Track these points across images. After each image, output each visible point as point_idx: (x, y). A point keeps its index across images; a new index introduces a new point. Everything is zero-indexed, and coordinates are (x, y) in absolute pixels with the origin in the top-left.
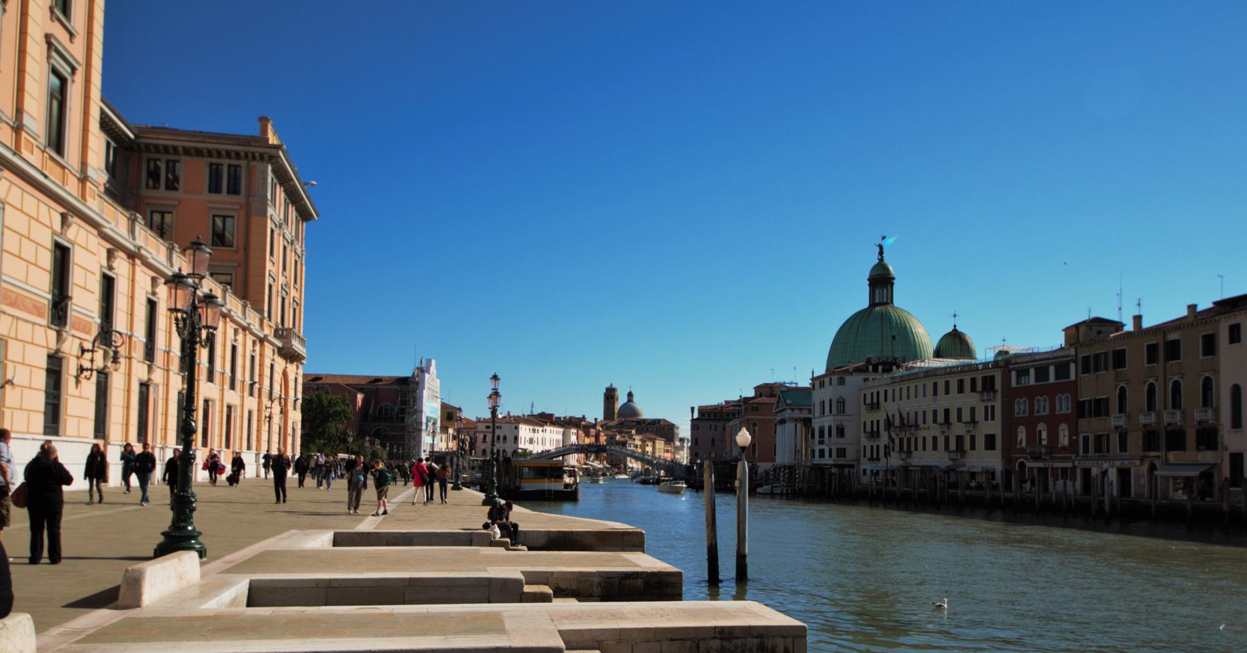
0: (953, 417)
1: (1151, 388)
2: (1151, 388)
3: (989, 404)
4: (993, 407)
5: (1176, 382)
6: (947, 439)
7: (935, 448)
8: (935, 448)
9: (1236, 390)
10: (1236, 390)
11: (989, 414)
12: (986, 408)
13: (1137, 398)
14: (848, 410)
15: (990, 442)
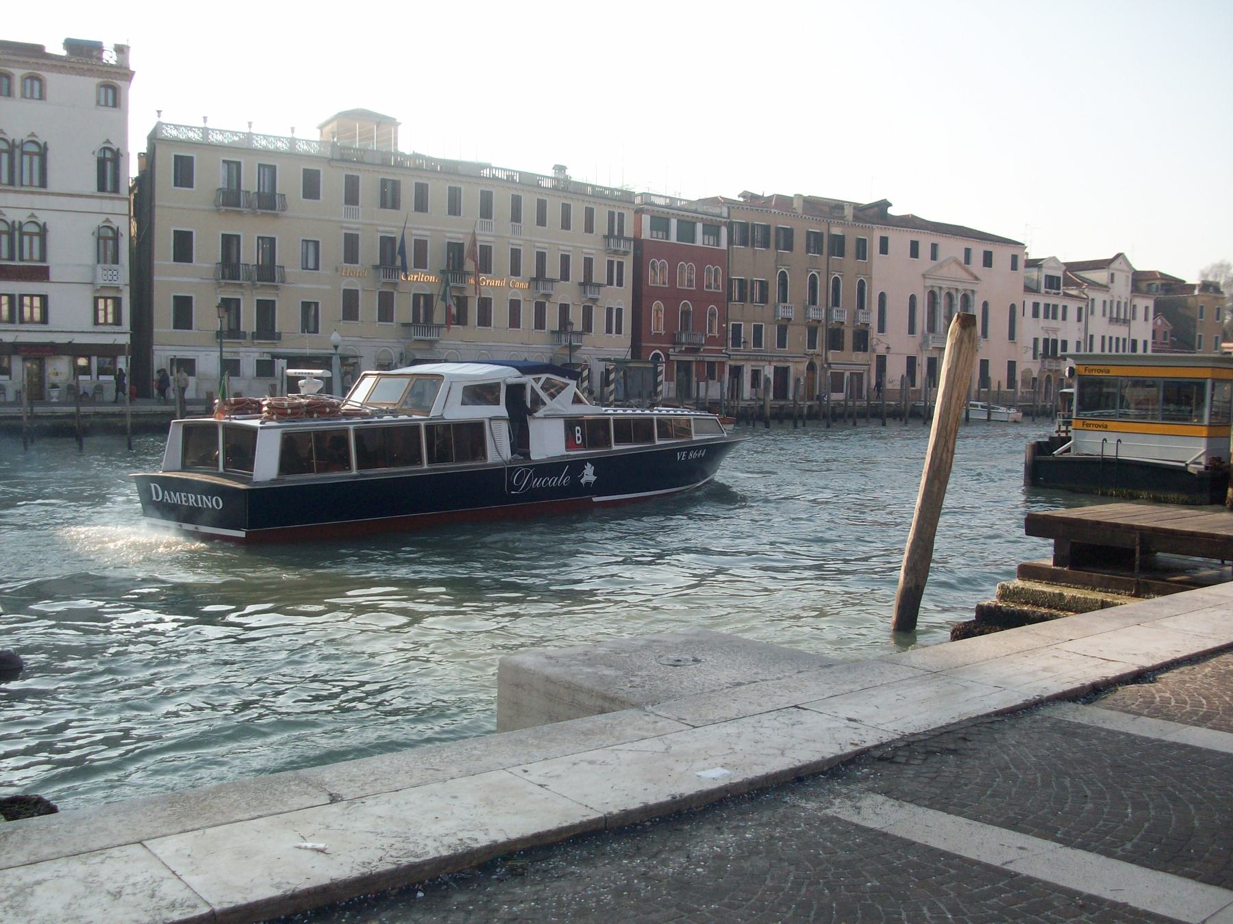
0: (553, 270)
1: (813, 280)
2: (813, 280)
3: (616, 259)
4: (620, 265)
5: (836, 278)
6: (540, 309)
7: (515, 322)
8: (515, 322)
9: (882, 296)
10: (882, 296)
11: (615, 275)
12: (610, 263)
13: (798, 289)
14: (55, 180)
15: (613, 321)
